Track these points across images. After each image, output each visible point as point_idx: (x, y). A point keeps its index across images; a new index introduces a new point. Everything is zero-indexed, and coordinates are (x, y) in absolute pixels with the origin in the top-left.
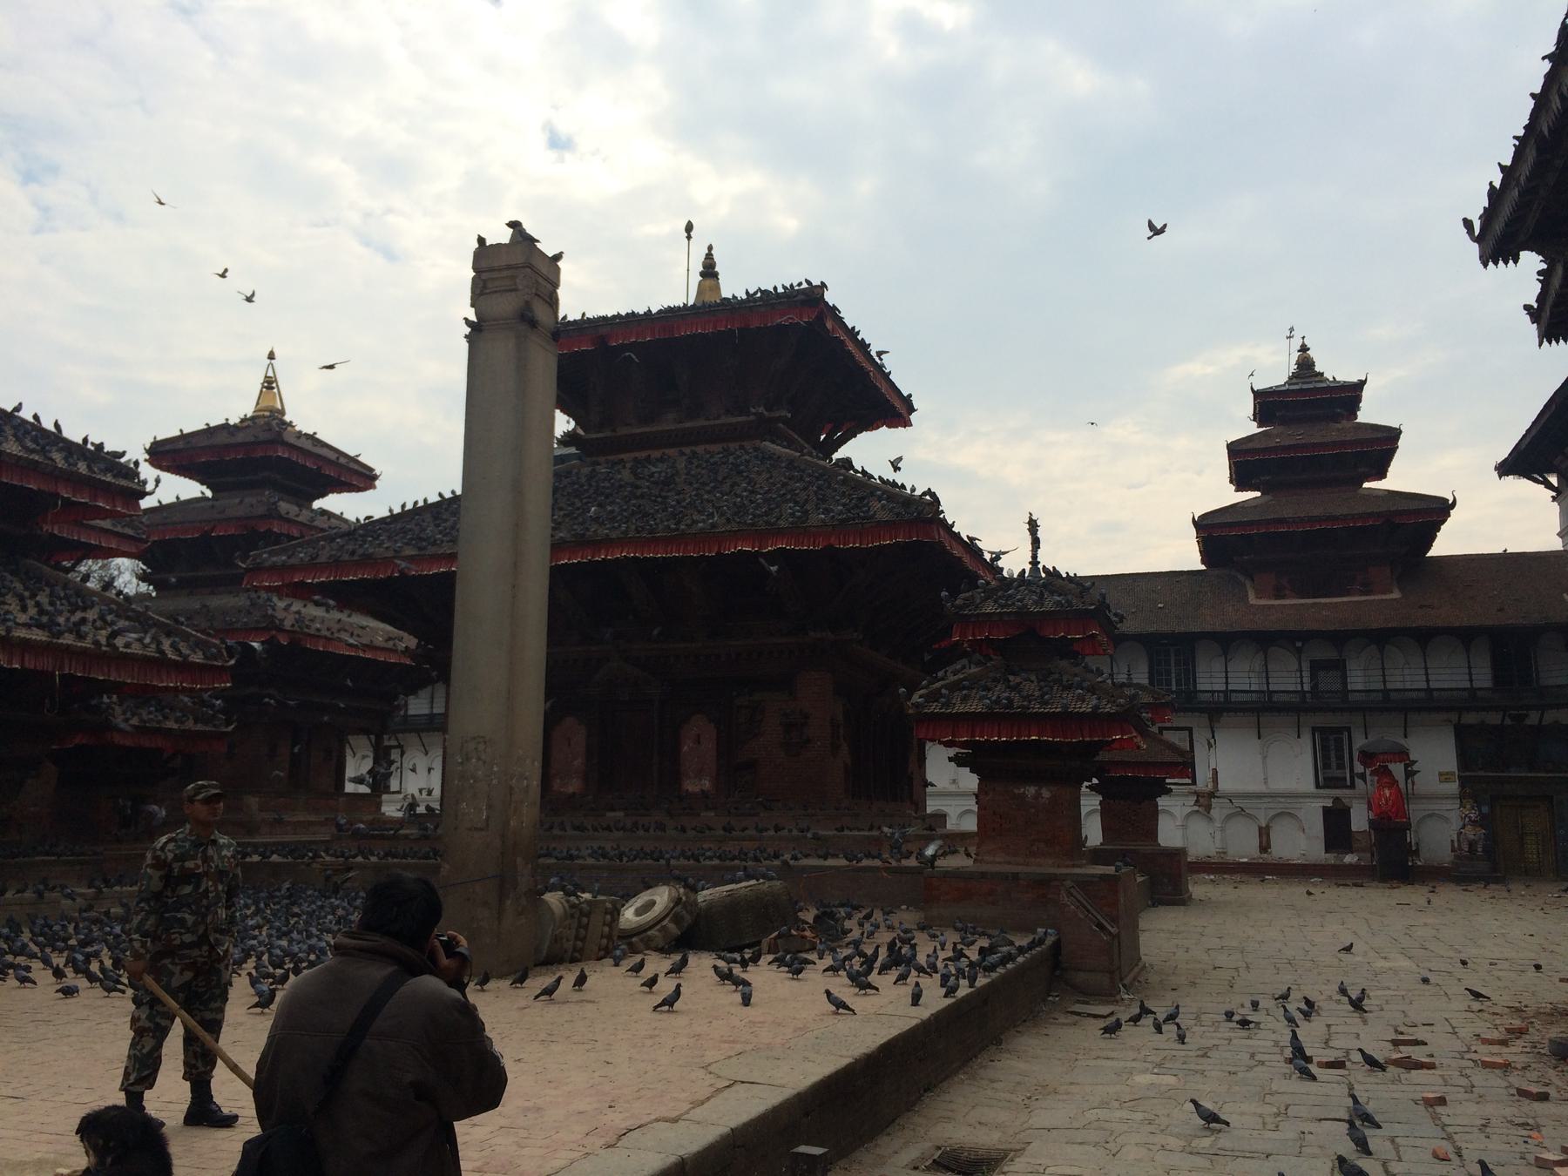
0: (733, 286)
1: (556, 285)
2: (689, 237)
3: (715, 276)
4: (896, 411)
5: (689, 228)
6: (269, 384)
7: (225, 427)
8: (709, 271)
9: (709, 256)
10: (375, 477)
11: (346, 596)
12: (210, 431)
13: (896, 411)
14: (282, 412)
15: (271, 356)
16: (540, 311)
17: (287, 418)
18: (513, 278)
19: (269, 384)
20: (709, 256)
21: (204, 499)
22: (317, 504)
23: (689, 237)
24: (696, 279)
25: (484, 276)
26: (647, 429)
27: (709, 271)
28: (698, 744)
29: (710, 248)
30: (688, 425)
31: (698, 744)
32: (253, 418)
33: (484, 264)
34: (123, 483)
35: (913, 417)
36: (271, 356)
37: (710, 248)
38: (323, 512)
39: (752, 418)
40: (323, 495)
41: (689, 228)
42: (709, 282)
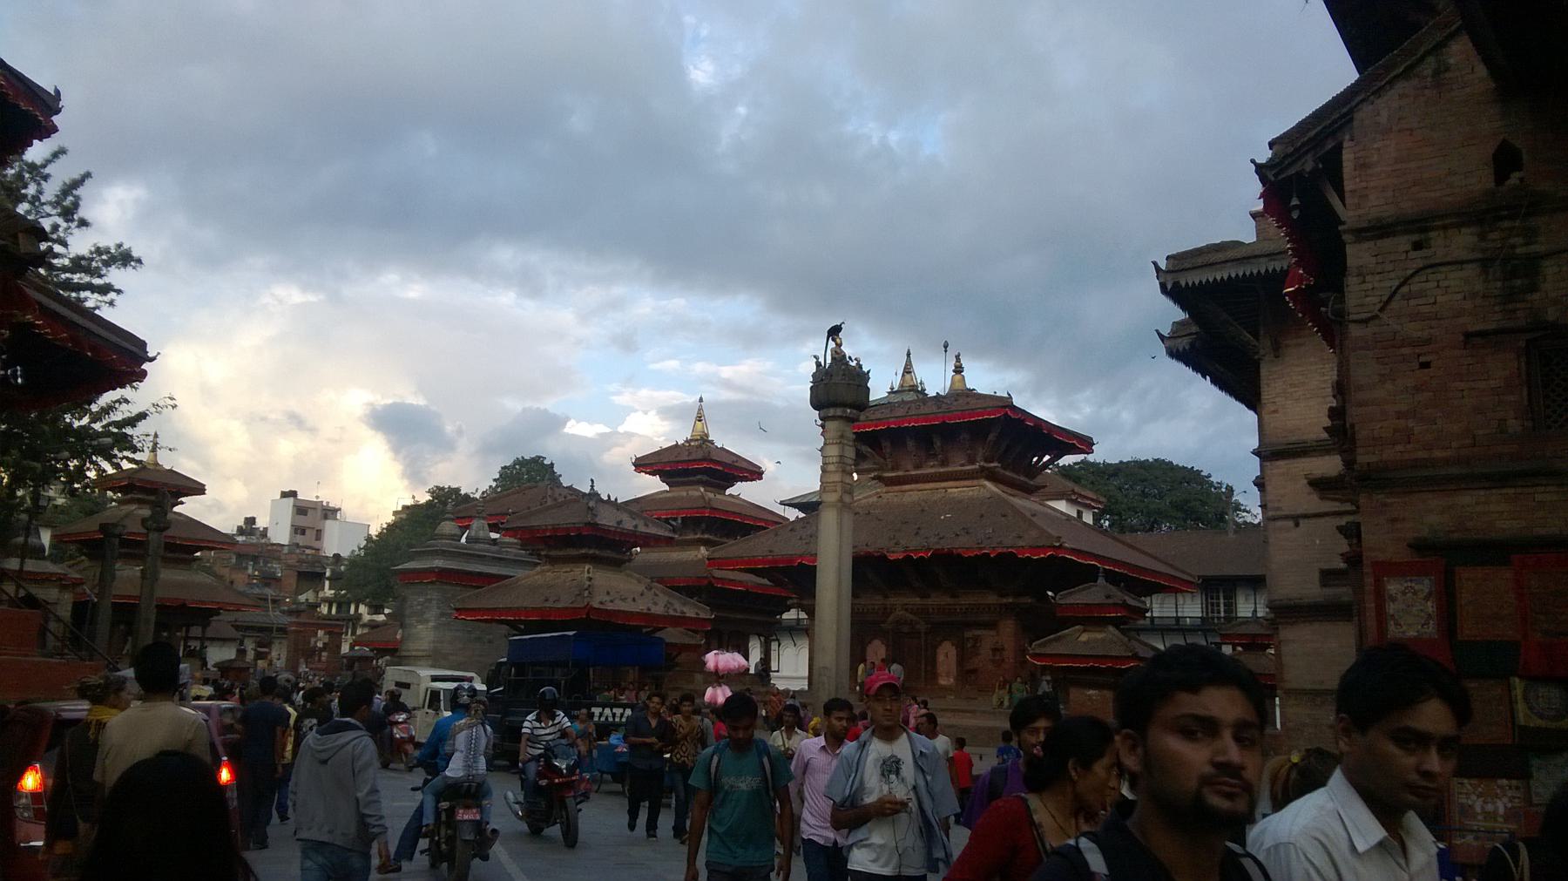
5: (946, 346)
22: (728, 492)
28: (947, 655)
31: (947, 655)
41: (946, 346)
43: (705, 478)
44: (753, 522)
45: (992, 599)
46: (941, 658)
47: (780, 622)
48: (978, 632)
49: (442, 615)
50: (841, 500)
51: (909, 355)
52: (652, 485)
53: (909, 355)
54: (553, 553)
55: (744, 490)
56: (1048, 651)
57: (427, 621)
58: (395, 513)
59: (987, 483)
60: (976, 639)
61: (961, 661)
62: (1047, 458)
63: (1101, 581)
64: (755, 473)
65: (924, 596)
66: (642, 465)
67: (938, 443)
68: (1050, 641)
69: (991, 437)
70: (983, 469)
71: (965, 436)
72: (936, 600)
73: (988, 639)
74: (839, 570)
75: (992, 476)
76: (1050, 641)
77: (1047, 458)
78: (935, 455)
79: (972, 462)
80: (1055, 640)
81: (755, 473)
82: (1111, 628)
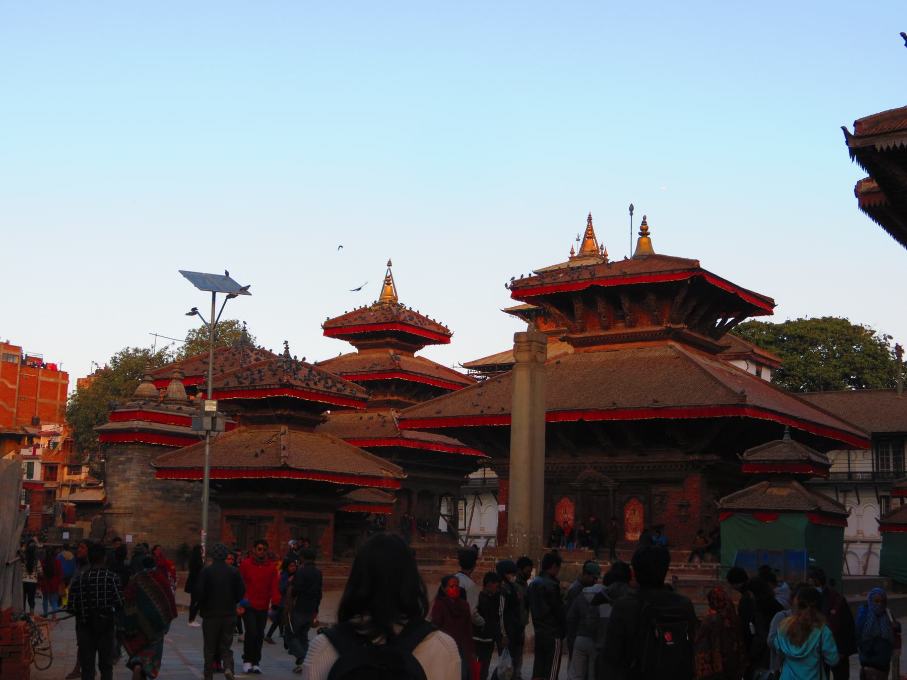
2: (631, 214)
5: (632, 208)
6: (388, 281)
9: (644, 223)
10: (450, 335)
11: (448, 432)
14: (396, 299)
15: (389, 264)
16: (540, 358)
19: (388, 281)
20: (644, 223)
21: (355, 354)
22: (417, 354)
23: (631, 214)
24: (636, 236)
26: (607, 333)
29: (645, 218)
30: (630, 331)
32: (379, 304)
35: (774, 310)
36: (389, 264)
37: (645, 218)
38: (419, 357)
40: (420, 348)
41: (632, 208)
42: (644, 240)
43: (394, 340)
44: (440, 383)
47: (468, 481)
49: (143, 473)
50: (534, 359)
51: (590, 219)
52: (345, 348)
53: (590, 219)
55: (430, 353)
56: (735, 505)
57: (128, 480)
58: (136, 350)
59: (672, 343)
61: (648, 518)
62: (730, 320)
63: (786, 437)
64: (442, 336)
66: (333, 329)
67: (626, 304)
68: (739, 496)
69: (679, 299)
70: (669, 331)
74: (532, 427)
75: (679, 337)
76: (739, 496)
77: (730, 320)
78: (623, 318)
79: (659, 323)
80: (744, 494)
81: (442, 336)
82: (795, 484)
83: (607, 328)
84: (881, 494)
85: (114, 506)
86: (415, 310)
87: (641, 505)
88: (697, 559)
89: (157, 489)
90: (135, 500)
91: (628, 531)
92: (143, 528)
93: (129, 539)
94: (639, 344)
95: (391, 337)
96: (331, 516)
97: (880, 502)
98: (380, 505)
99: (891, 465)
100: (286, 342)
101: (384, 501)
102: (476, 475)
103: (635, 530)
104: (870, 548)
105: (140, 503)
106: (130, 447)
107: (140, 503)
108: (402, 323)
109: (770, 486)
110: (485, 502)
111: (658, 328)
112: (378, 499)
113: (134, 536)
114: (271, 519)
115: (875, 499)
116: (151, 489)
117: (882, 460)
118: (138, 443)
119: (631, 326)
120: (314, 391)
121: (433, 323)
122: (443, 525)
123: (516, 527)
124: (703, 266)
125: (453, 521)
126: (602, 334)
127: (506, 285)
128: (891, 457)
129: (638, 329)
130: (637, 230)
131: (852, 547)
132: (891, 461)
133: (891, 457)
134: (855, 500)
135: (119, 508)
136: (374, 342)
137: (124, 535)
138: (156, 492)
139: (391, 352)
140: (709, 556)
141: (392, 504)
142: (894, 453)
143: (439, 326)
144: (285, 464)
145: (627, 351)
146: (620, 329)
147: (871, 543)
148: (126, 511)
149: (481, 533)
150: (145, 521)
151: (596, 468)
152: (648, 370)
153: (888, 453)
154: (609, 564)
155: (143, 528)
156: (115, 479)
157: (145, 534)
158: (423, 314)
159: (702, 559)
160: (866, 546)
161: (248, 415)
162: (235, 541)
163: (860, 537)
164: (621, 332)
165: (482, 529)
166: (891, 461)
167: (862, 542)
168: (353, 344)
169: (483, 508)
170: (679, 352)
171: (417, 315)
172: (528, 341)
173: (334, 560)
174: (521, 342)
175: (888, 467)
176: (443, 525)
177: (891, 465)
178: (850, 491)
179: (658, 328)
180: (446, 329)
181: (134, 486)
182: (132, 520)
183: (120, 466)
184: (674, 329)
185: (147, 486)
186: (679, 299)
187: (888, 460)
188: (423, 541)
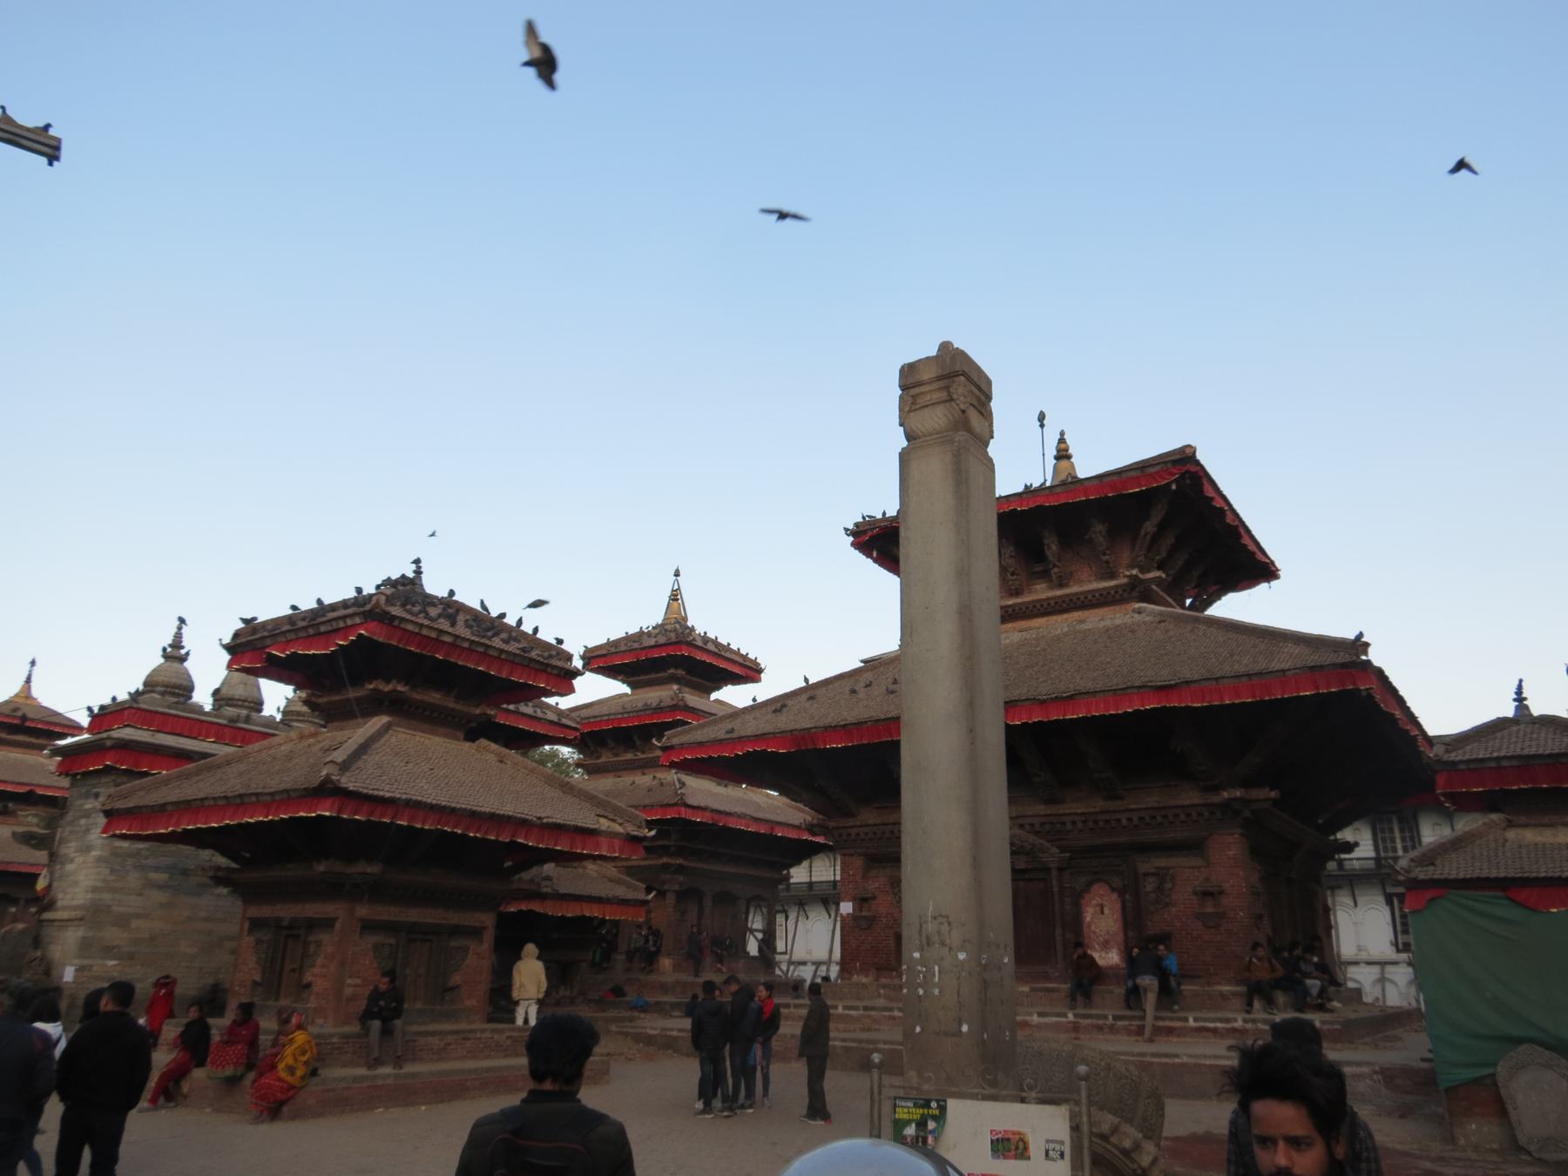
0: (1087, 466)
1: (989, 398)
2: (1042, 426)
3: (1069, 457)
4: (1263, 571)
5: (1042, 417)
6: (675, 596)
7: (641, 633)
8: (1063, 455)
9: (1062, 440)
10: (760, 671)
12: (628, 638)
13: (1263, 571)
14: (685, 619)
15: (677, 574)
17: (689, 624)
18: (947, 388)
19: (675, 596)
20: (1062, 440)
22: (714, 696)
23: (1042, 426)
24: (1051, 462)
25: (914, 391)
27: (1063, 455)
29: (1062, 433)
32: (662, 625)
33: (911, 381)
34: (560, 664)
36: (677, 574)
37: (1062, 433)
38: (717, 701)
39: (1125, 580)
40: (718, 688)
41: (1042, 417)
42: (1064, 463)
43: (680, 672)
45: (1190, 797)
46: (1089, 914)
48: (1161, 862)
54: (320, 701)
55: (735, 696)
57: (87, 849)
59: (1137, 605)
60: (1161, 875)
61: (1133, 920)
64: (749, 672)
65: (1050, 801)
67: (1052, 547)
69: (1150, 527)
70: (1134, 583)
71: (1098, 530)
72: (1075, 807)
73: (1187, 874)
78: (1045, 575)
79: (1112, 575)
83: (1017, 593)
84: (1390, 890)
85: (60, 904)
86: (711, 635)
87: (1115, 896)
88: (1257, 1004)
89: (156, 869)
90: (95, 889)
91: (1093, 948)
92: (108, 951)
93: (69, 975)
94: (1076, 615)
95: (676, 668)
96: (487, 920)
97: (1389, 902)
98: (623, 902)
99: (1399, 846)
100: (417, 561)
101: (631, 895)
102: (799, 874)
103: (1106, 945)
104: (1383, 972)
105: (106, 896)
106: (104, 780)
107: (106, 896)
108: (691, 644)
109: (1511, 825)
110: (811, 915)
111: (1112, 583)
112: (621, 892)
113: (80, 970)
114: (328, 924)
115: (1381, 899)
116: (140, 867)
117: (1384, 840)
118: (107, 770)
119: (1061, 586)
120: (447, 639)
121: (738, 653)
122: (753, 948)
123: (931, 927)
124: (1199, 456)
125: (768, 942)
126: (1010, 602)
127: (846, 530)
128: (1397, 834)
129: (1074, 589)
130: (1051, 452)
131: (1353, 972)
132: (1398, 840)
133: (1397, 834)
134: (1349, 901)
135: (65, 908)
136: (653, 676)
137: (64, 965)
138: (153, 875)
139: (675, 687)
140: (1280, 997)
141: (644, 903)
142: (1402, 830)
143: (745, 657)
144: (327, 780)
145: (1059, 624)
146: (1041, 592)
147: (1383, 964)
148: (73, 914)
149: (808, 957)
150: (113, 935)
151: (1021, 826)
152: (1110, 645)
153: (1391, 831)
154: (1071, 1017)
155: (108, 951)
156: (70, 849)
157: (111, 963)
158: (723, 641)
159: (1270, 1002)
160: (1376, 969)
161: (320, 701)
162: (258, 978)
163: (1364, 956)
164: (1043, 596)
165: (809, 952)
166: (1398, 840)
167: (1369, 963)
168: (624, 682)
169: (809, 923)
170: (1161, 614)
171: (715, 642)
172: (940, 378)
173: (490, 1020)
174: (920, 384)
175: (1395, 850)
176: (753, 948)
177: (1399, 846)
178: (1340, 887)
179: (1112, 583)
180: (755, 662)
181: (99, 860)
182: (81, 932)
183: (83, 821)
184: (1142, 581)
185: (130, 862)
186: (1150, 527)
187: (1393, 840)
188: (720, 970)
